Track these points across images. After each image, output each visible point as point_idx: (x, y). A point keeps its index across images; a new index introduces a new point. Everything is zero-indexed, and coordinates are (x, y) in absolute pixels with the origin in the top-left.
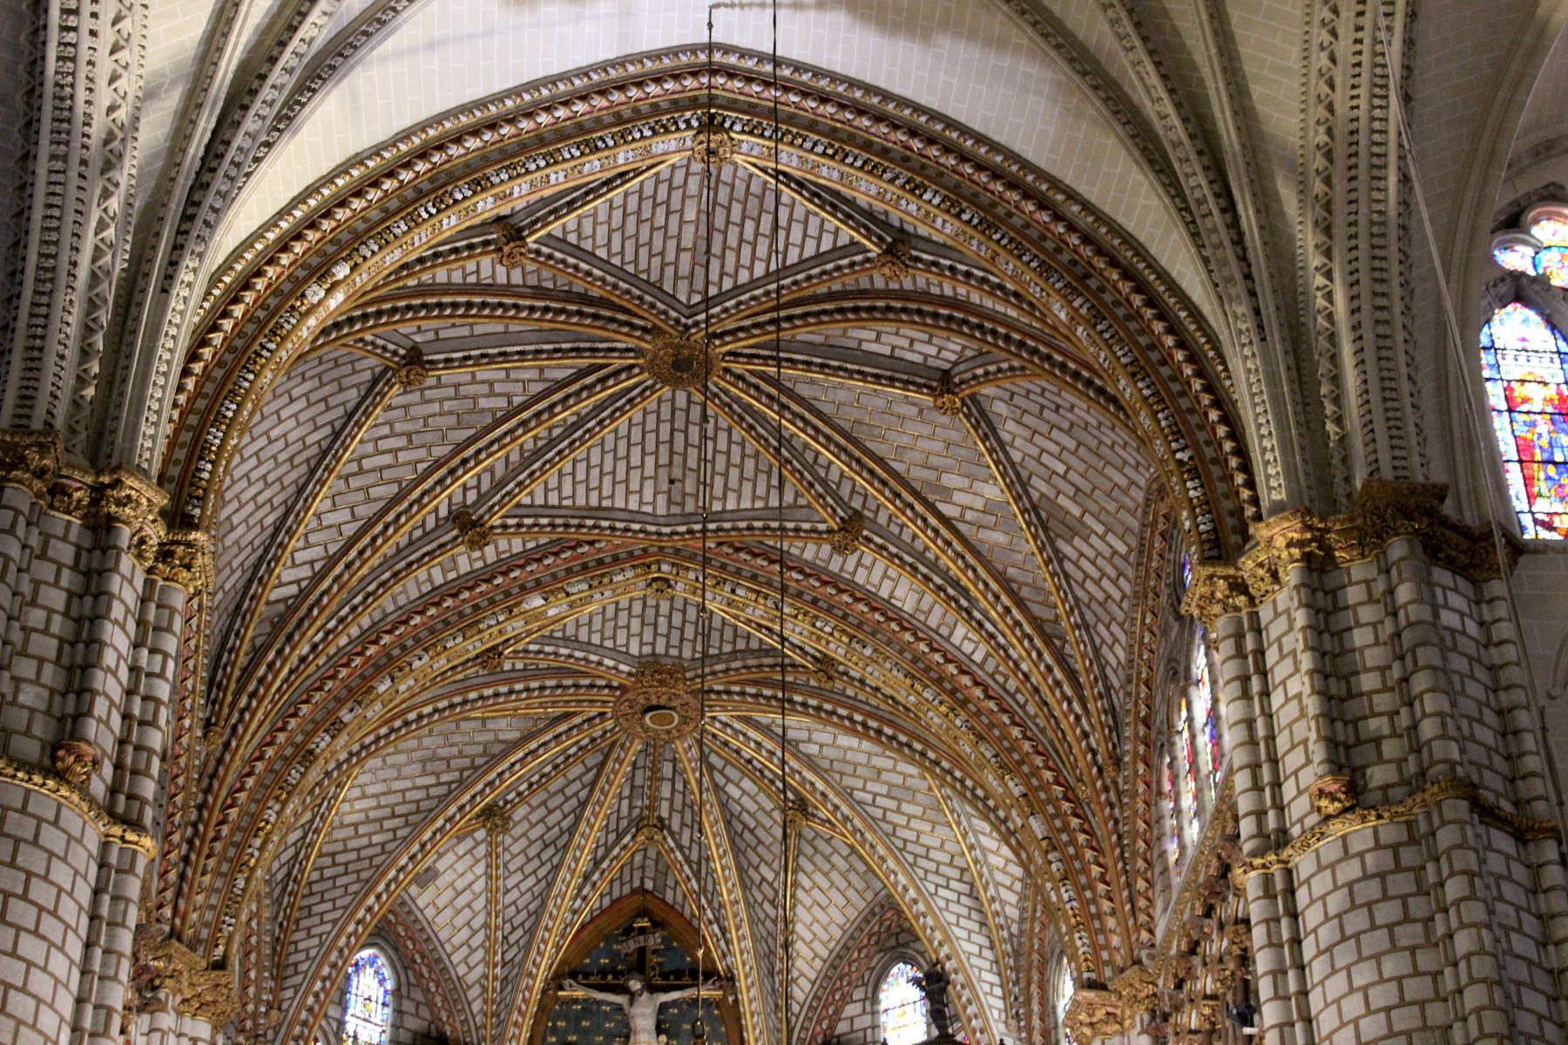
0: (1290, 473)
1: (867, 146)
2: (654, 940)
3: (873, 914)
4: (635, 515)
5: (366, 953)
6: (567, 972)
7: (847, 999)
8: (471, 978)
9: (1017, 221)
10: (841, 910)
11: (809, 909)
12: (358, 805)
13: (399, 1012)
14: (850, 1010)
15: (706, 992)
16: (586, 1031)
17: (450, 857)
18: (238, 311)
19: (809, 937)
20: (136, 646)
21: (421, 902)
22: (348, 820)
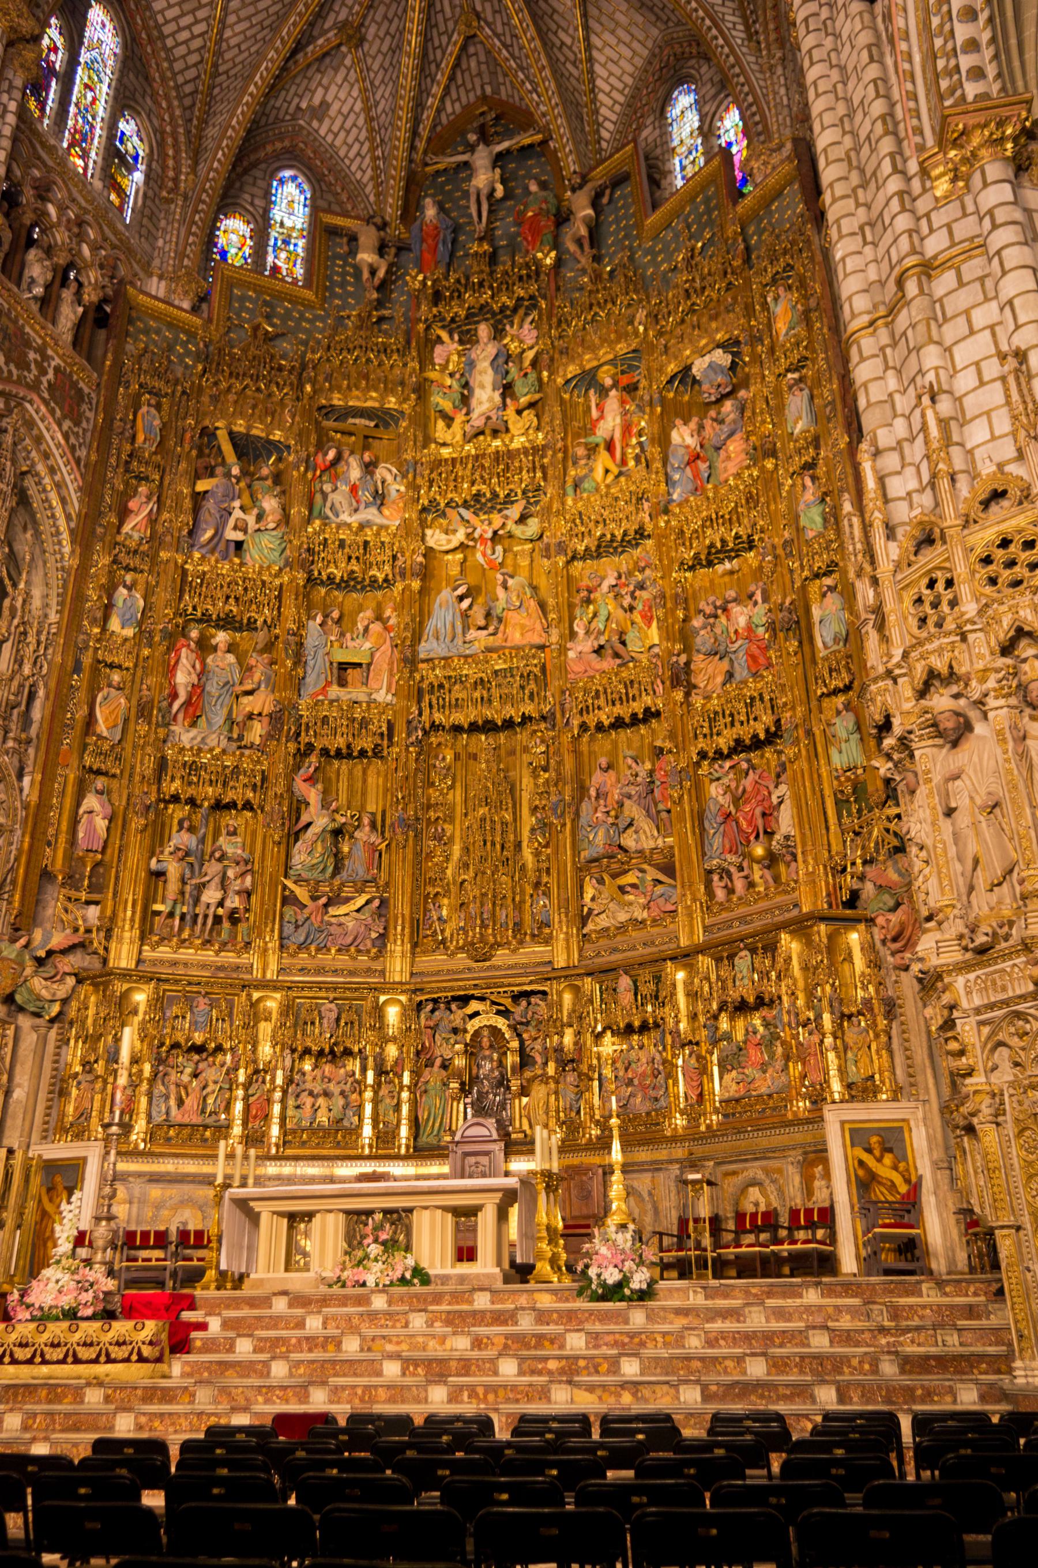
3: (654, 55)
5: (287, 173)
8: (365, 180)
10: (630, 61)
11: (604, 66)
12: (238, 28)
16: (450, 192)
17: (333, 89)
19: (607, 89)
21: (322, 132)
22: (233, 42)
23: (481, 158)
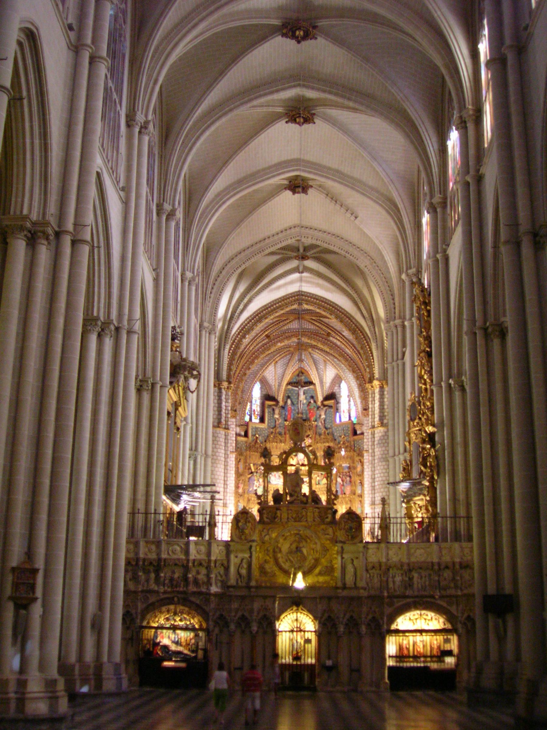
0: (379, 373)
1: (323, 307)
2: (303, 378)
4: (294, 329)
6: (289, 383)
7: (335, 386)
9: (345, 321)
13: (261, 391)
14: (336, 388)
15: (312, 387)
18: (233, 346)
20: (226, 402)
23: (301, 393)
